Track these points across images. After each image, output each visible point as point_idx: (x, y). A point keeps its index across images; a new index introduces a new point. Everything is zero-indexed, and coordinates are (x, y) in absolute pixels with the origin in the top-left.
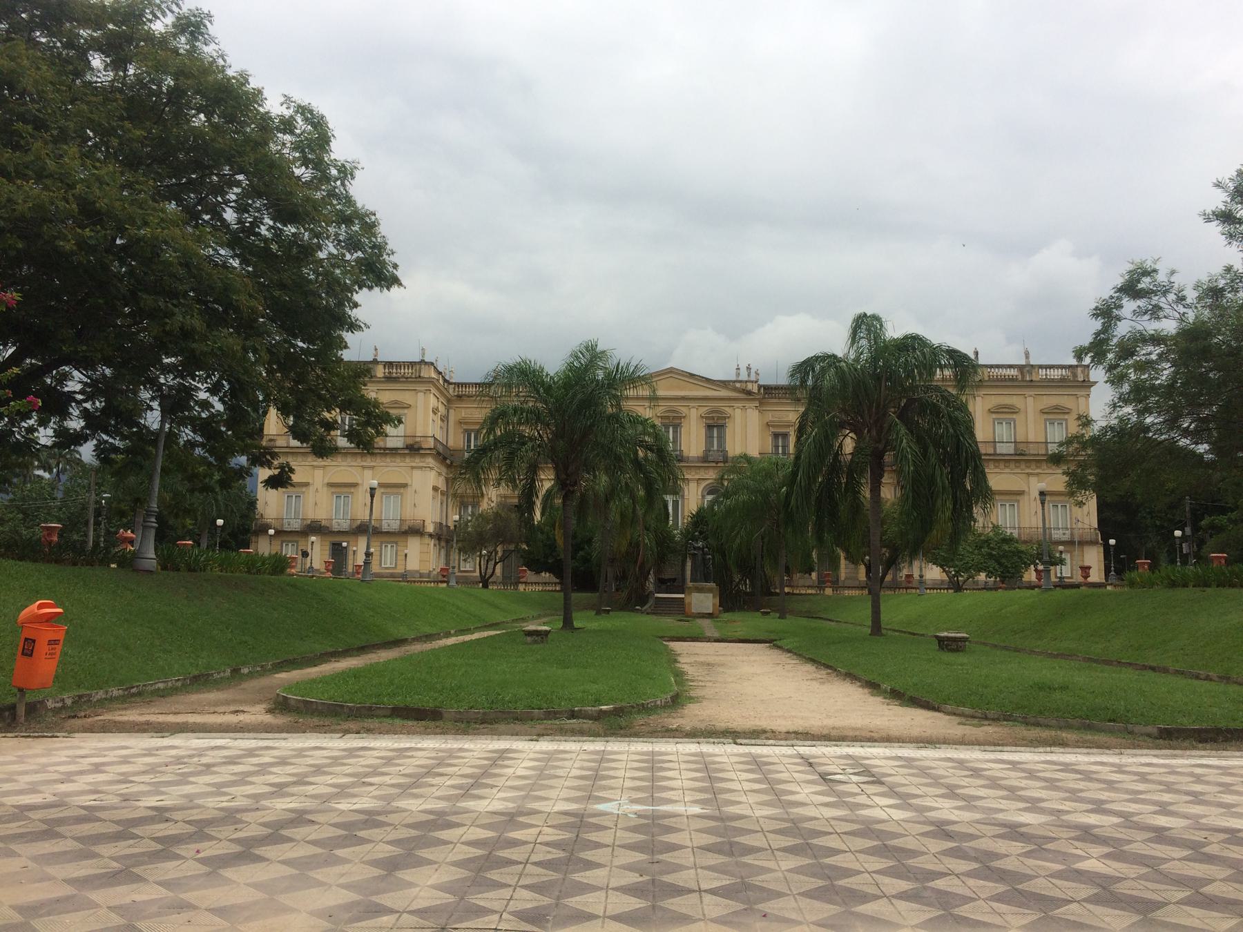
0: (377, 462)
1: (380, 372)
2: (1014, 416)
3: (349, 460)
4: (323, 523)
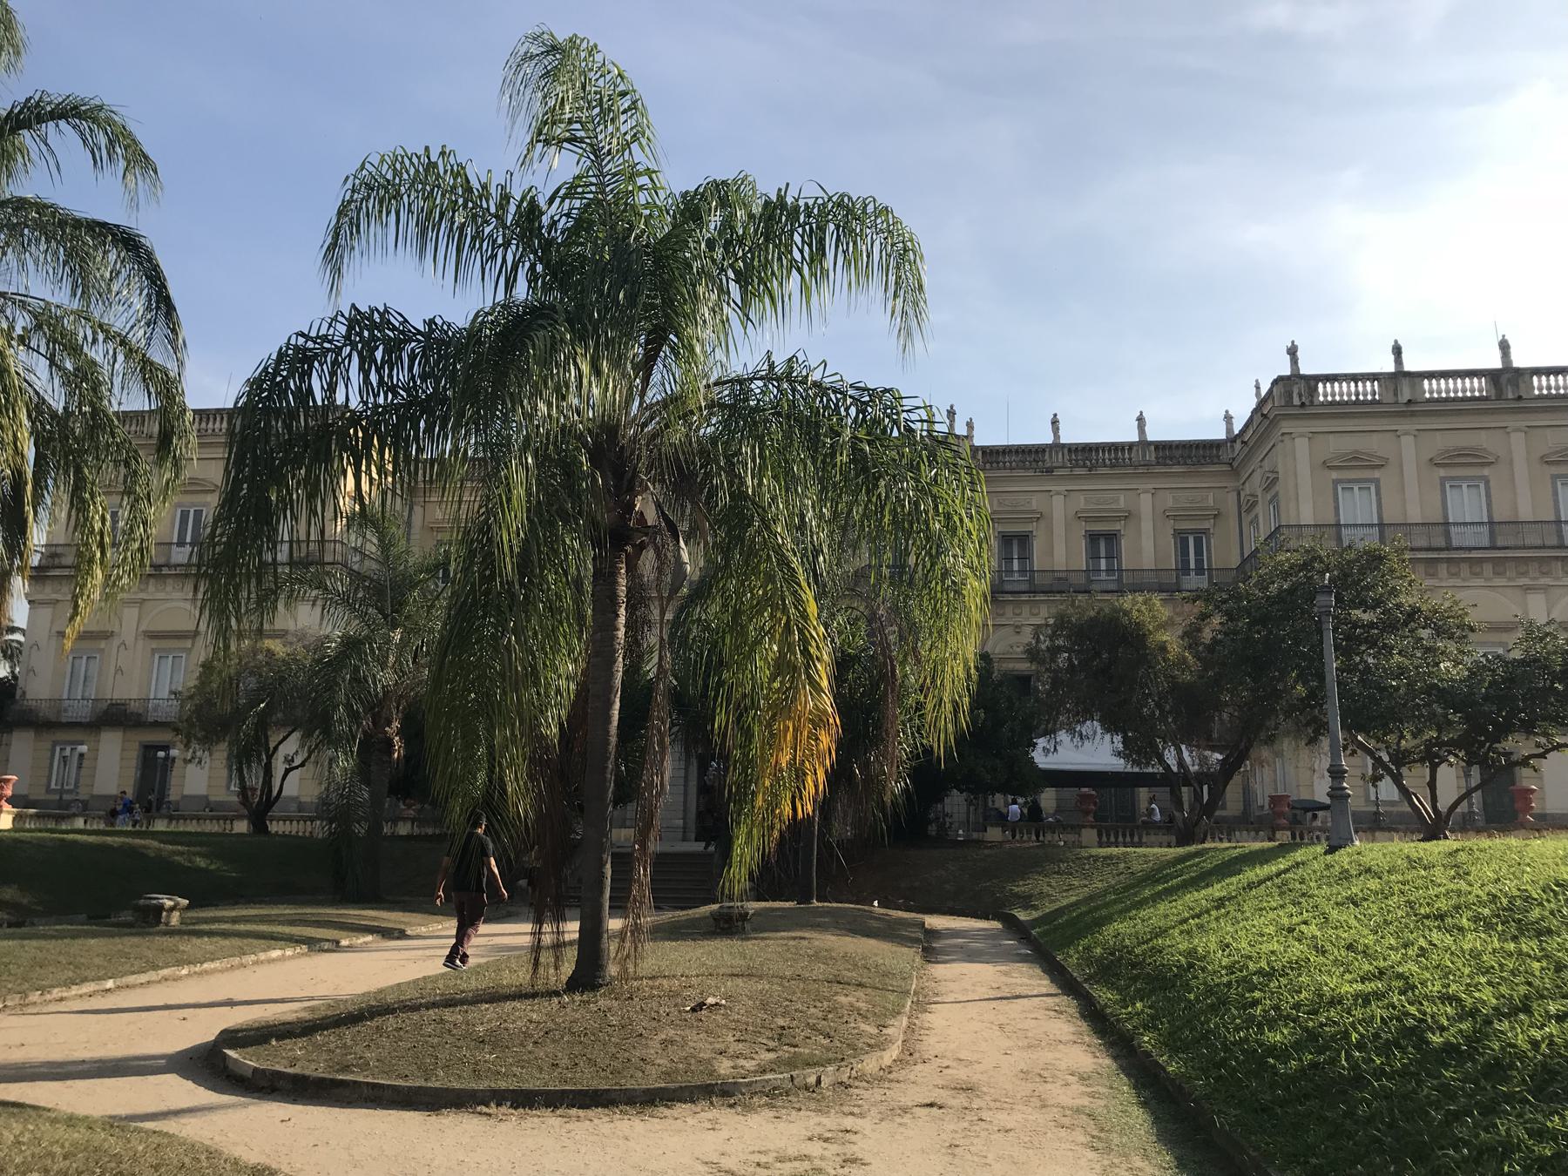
2: (1486, 472)
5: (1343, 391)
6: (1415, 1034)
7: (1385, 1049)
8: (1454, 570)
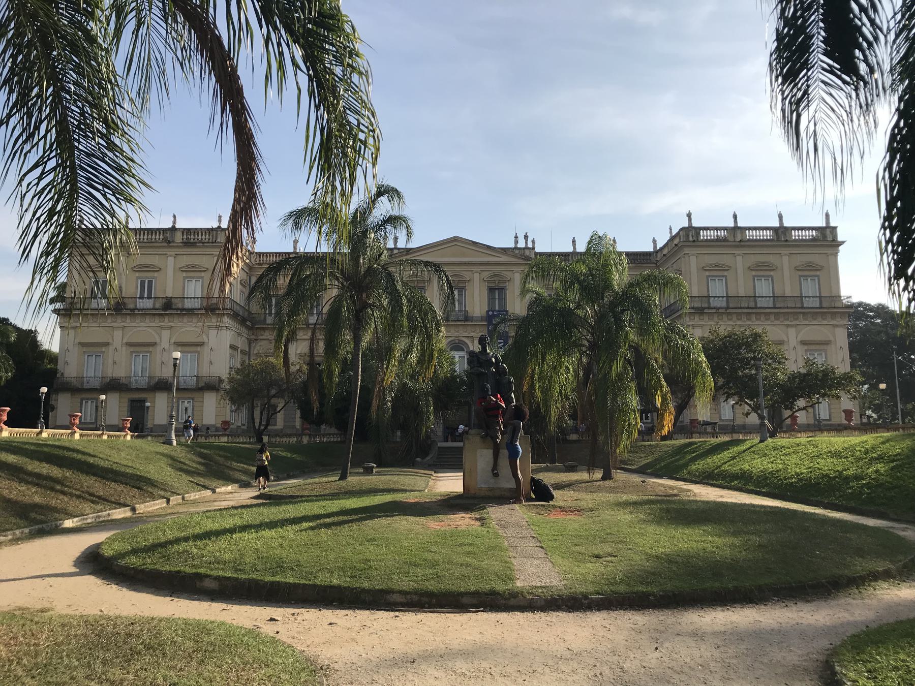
0: (176, 322)
1: (179, 238)
2: (772, 273)
4: (124, 381)
5: (712, 234)
6: (827, 475)
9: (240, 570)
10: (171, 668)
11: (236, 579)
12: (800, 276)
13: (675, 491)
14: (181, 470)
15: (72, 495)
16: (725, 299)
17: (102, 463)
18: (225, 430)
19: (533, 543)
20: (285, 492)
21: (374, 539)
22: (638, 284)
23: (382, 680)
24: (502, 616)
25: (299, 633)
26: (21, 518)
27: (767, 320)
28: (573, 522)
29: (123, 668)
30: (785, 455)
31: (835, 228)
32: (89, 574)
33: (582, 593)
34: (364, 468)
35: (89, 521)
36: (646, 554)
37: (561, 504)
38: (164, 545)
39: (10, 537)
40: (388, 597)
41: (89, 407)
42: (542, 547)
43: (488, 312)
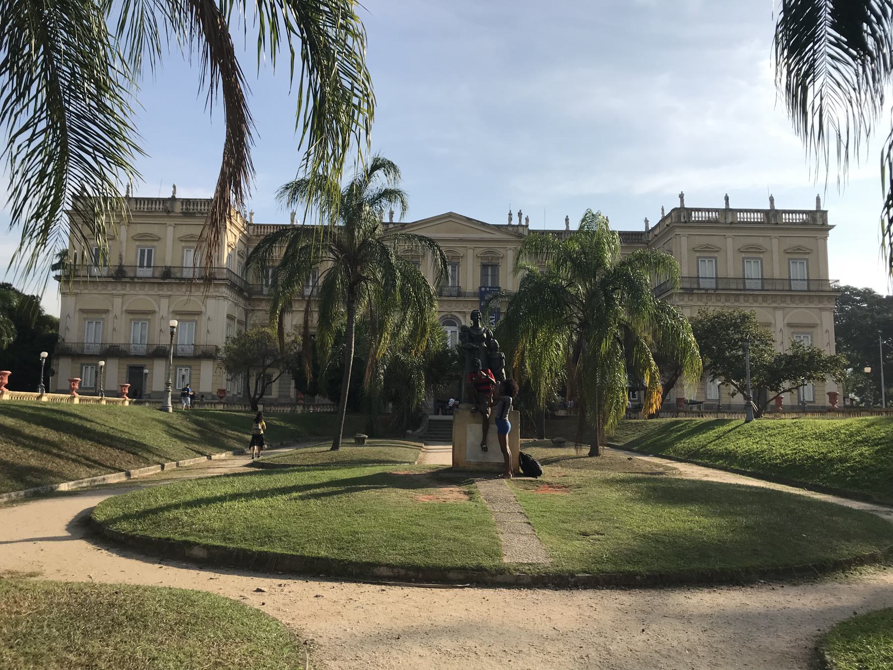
1: (178, 208)
2: (761, 256)
3: (147, 287)
4: (123, 348)
5: (703, 216)
6: (811, 457)
7: (806, 460)
8: (746, 299)
9: (229, 539)
10: (151, 641)
11: (225, 548)
12: (789, 259)
13: (661, 469)
14: (176, 436)
15: (68, 459)
16: (714, 280)
17: (98, 428)
18: (221, 398)
19: (521, 519)
20: (277, 461)
21: (362, 511)
22: (630, 263)
23: (366, 657)
24: (488, 593)
25: (284, 605)
26: (17, 481)
27: (756, 301)
28: (560, 498)
29: (102, 640)
30: (770, 435)
31: (825, 213)
32: (81, 539)
33: (568, 571)
34: (356, 439)
35: (84, 485)
36: (634, 533)
37: (549, 480)
38: (155, 511)
39: (5, 499)
40: (375, 570)
41: (89, 372)
42: (529, 523)
43: (480, 288)
